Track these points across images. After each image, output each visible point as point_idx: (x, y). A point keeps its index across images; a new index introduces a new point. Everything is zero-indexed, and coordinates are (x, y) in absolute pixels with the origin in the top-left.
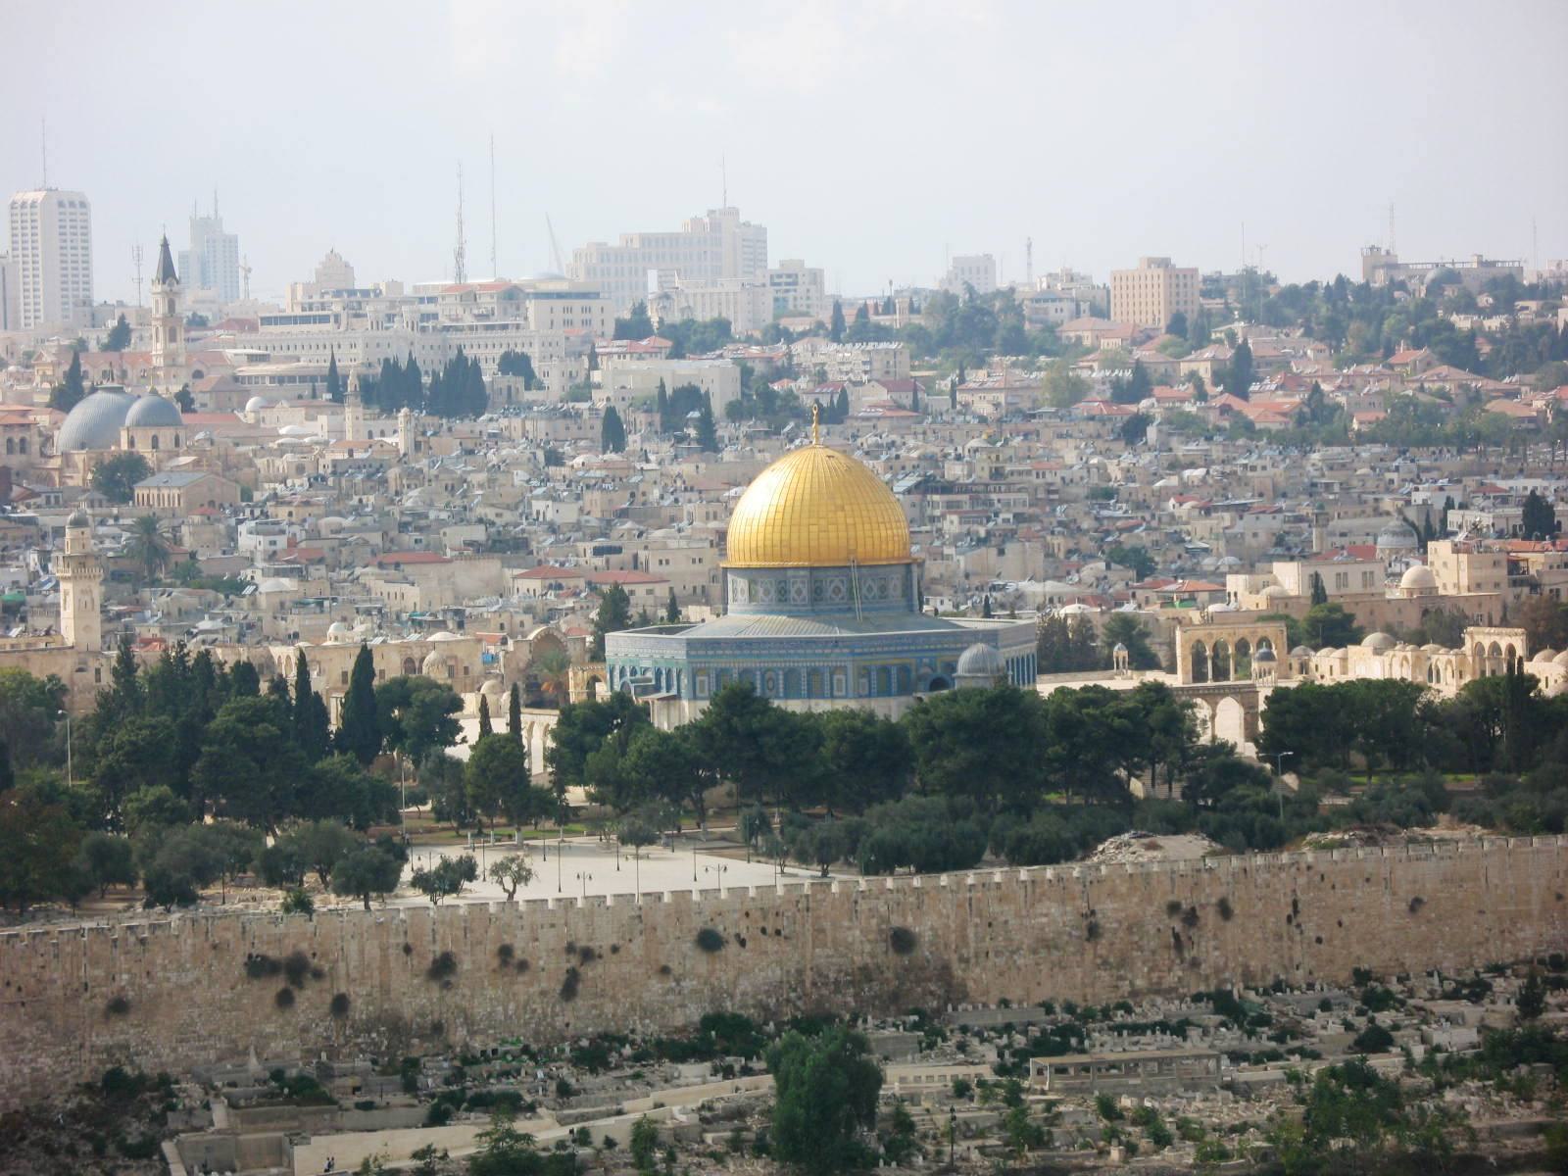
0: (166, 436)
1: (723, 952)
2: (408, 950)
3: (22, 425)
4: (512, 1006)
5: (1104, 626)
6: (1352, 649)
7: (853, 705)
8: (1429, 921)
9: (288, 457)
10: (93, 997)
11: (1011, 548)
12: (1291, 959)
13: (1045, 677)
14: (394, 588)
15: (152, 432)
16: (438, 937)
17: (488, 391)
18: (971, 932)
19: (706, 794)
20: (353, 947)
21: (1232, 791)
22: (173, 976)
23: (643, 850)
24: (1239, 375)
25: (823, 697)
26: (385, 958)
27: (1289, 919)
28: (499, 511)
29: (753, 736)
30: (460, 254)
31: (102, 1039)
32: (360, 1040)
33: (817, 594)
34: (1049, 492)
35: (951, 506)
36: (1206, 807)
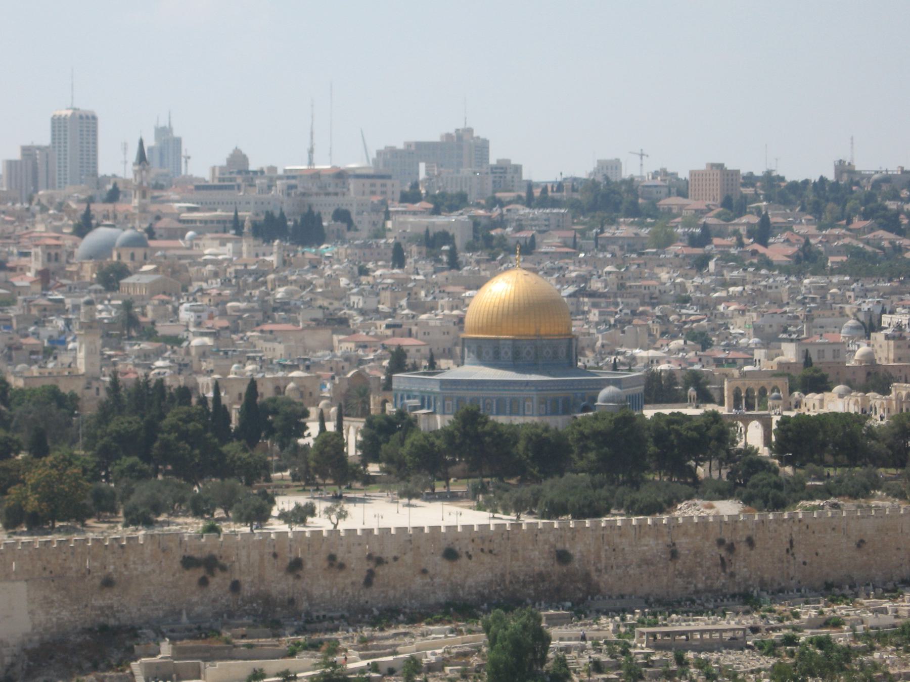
0: (139, 252)
1: (459, 562)
2: (275, 555)
3: (57, 245)
4: (335, 591)
5: (682, 377)
6: (827, 395)
7: (536, 419)
8: (868, 554)
9: (210, 267)
10: (93, 578)
12: (788, 574)
13: (648, 406)
14: (269, 345)
15: (131, 250)
16: (293, 550)
17: (326, 231)
18: (603, 555)
19: (450, 470)
20: (244, 553)
21: (756, 476)
22: (140, 568)
23: (414, 501)
24: (763, 233)
25: (517, 414)
27: (788, 551)
28: (332, 301)
30: (311, 152)
31: (99, 602)
32: (246, 608)
33: (516, 354)
35: (595, 305)
36: (740, 484)
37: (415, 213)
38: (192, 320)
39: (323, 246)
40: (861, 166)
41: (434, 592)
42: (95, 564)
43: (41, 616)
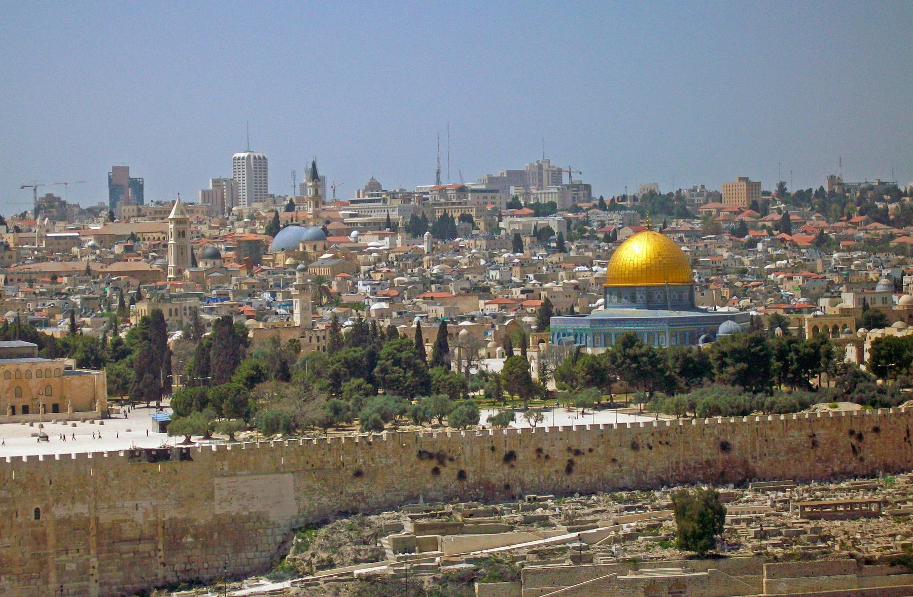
0: (320, 245)
1: (641, 452)
2: (493, 449)
4: (542, 478)
9: (375, 255)
10: (347, 469)
11: (705, 292)
12: (906, 458)
14: (431, 308)
16: (507, 444)
18: (757, 445)
20: (468, 448)
22: (384, 461)
26: (482, 454)
27: (905, 439)
29: (635, 359)
30: (438, 173)
31: (352, 490)
34: (718, 270)
37: (520, 216)
38: (369, 291)
39: (457, 239)
40: (849, 179)
41: (622, 478)
42: (348, 458)
43: (306, 503)
